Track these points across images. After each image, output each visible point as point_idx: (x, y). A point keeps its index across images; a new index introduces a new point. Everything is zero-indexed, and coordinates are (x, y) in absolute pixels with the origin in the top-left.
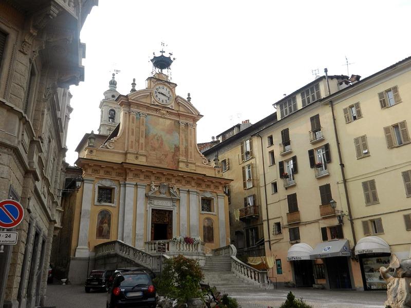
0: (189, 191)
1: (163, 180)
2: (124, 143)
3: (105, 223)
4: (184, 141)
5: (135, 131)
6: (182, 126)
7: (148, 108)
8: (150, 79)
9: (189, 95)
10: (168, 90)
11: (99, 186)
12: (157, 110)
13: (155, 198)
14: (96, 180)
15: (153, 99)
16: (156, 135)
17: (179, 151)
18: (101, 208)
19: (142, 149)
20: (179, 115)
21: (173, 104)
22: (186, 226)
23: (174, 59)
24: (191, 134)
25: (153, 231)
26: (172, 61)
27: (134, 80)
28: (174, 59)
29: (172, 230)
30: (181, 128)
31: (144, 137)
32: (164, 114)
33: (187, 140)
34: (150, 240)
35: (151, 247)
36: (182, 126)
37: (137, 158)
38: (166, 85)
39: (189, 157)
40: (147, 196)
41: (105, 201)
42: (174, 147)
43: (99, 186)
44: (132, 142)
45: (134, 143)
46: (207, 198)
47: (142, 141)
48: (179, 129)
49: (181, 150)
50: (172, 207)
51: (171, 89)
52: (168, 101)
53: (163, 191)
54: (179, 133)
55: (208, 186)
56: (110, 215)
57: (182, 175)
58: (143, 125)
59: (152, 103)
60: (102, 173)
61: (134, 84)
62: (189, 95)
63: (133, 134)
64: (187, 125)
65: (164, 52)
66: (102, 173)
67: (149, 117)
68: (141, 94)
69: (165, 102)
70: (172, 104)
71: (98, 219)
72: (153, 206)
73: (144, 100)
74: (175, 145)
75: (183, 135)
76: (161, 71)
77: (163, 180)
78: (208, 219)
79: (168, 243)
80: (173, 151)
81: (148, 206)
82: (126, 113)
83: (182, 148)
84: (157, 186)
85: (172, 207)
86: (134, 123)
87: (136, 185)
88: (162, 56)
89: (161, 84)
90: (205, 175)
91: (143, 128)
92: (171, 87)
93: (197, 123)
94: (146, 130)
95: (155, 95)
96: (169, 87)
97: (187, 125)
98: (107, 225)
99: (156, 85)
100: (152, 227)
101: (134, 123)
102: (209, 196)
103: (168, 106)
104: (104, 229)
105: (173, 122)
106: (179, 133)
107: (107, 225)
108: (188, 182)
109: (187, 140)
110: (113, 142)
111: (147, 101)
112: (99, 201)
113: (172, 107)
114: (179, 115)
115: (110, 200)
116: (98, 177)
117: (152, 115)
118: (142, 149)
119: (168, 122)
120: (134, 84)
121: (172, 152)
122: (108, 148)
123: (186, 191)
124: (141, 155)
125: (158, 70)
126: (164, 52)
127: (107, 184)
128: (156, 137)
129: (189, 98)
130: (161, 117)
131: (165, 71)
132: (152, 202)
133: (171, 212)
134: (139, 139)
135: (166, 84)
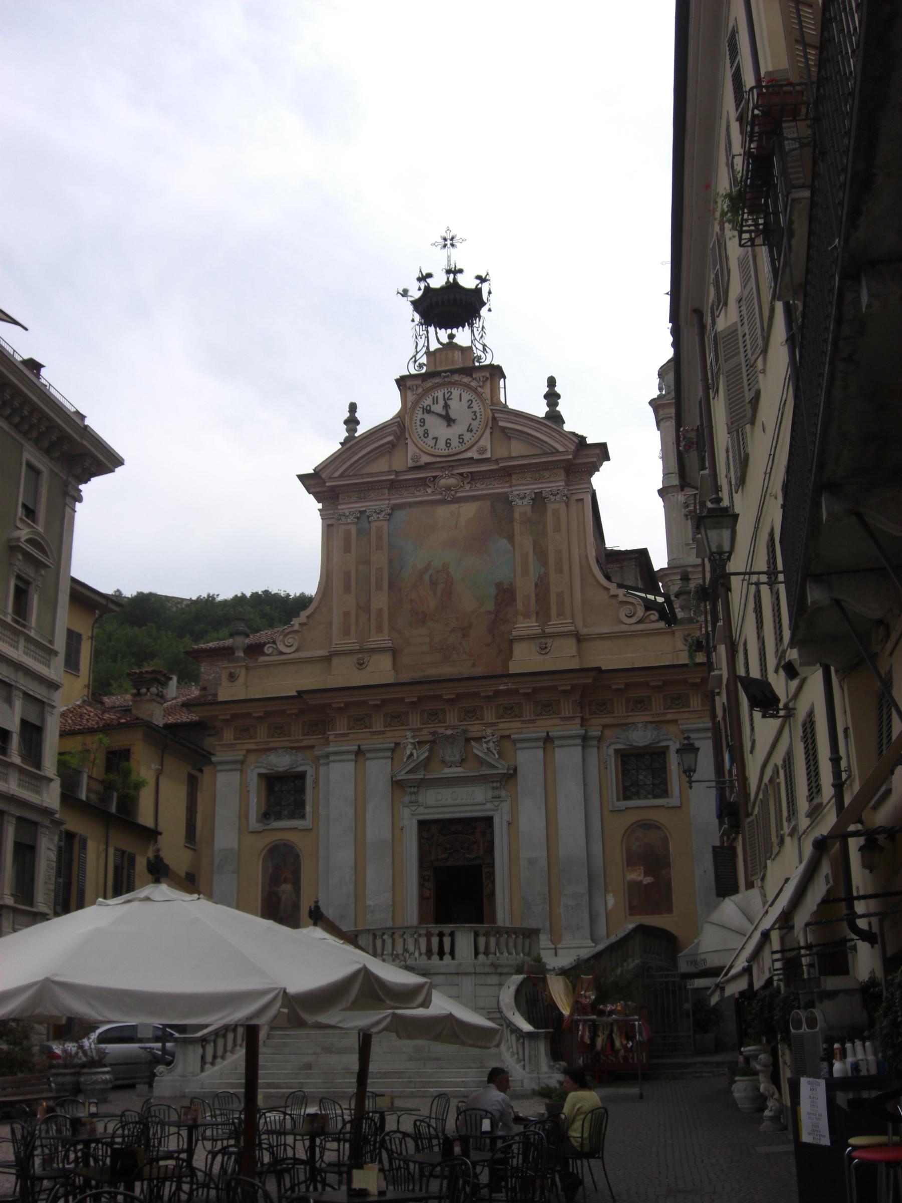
0: (548, 740)
1: (452, 718)
2: (331, 624)
3: (285, 881)
4: (531, 558)
5: (353, 575)
6: (522, 507)
7: (394, 486)
8: (402, 382)
9: (552, 382)
10: (466, 396)
11: (260, 775)
12: (423, 483)
13: (422, 784)
14: (251, 758)
15: (412, 449)
16: (427, 569)
17: (515, 600)
18: (269, 839)
19: (379, 629)
20: (506, 473)
21: (486, 441)
22: (543, 863)
23: (478, 277)
24: (557, 529)
25: (427, 893)
26: (478, 291)
27: (353, 408)
28: (482, 279)
29: (493, 882)
30: (517, 516)
31: (386, 586)
32: (448, 488)
33: (542, 555)
34: (415, 922)
35: (429, 944)
36: (522, 507)
37: (361, 665)
38: (454, 384)
39: (553, 613)
40: (397, 785)
41: (292, 816)
42: (493, 591)
43: (260, 775)
44: (346, 615)
45: (353, 617)
46: (637, 748)
47: (380, 601)
48: (511, 521)
49: (519, 597)
50: (489, 806)
51: (474, 390)
52: (467, 436)
53: (452, 753)
54: (511, 538)
55: (641, 704)
56: (297, 857)
57: (510, 686)
58: (379, 547)
59: (410, 463)
60: (262, 733)
61: (352, 422)
62: (552, 382)
63: (347, 589)
64: (539, 500)
65: (429, 275)
66: (262, 733)
67: (400, 515)
68: (362, 448)
69: (455, 442)
70: (482, 443)
71: (265, 869)
72: (421, 810)
73: (381, 466)
74: (499, 585)
75: (525, 542)
76: (451, 337)
77: (452, 718)
78: (647, 826)
79: (452, 935)
80: (490, 606)
81: (406, 812)
82: (332, 525)
83: (525, 587)
84: (426, 742)
85: (489, 806)
86: (350, 551)
87: (359, 752)
88: (428, 289)
89: (437, 386)
90: (599, 670)
91: (380, 560)
92: (474, 384)
93: (598, 481)
94: (390, 562)
95: (421, 431)
96: (467, 386)
97: (539, 500)
98: (287, 888)
99: (420, 398)
100: (422, 880)
101: (350, 551)
102: (647, 742)
103: (469, 455)
104: (283, 897)
105: (488, 503)
106: (511, 538)
107: (287, 888)
108: (548, 708)
109: (542, 555)
110: (296, 627)
111: (399, 462)
112: (266, 816)
113: (482, 451)
114: (506, 473)
115: (298, 810)
116: (252, 747)
117: (411, 505)
118: (379, 629)
119: (468, 511)
120: (352, 422)
121: (489, 612)
122: (282, 653)
123: (536, 740)
124: (373, 651)
125: (438, 337)
126: (429, 275)
127: (281, 762)
128: (427, 577)
129: (552, 397)
130: (443, 502)
131: (463, 336)
132: (421, 799)
133: (489, 820)
134: (369, 601)
135: (456, 377)
